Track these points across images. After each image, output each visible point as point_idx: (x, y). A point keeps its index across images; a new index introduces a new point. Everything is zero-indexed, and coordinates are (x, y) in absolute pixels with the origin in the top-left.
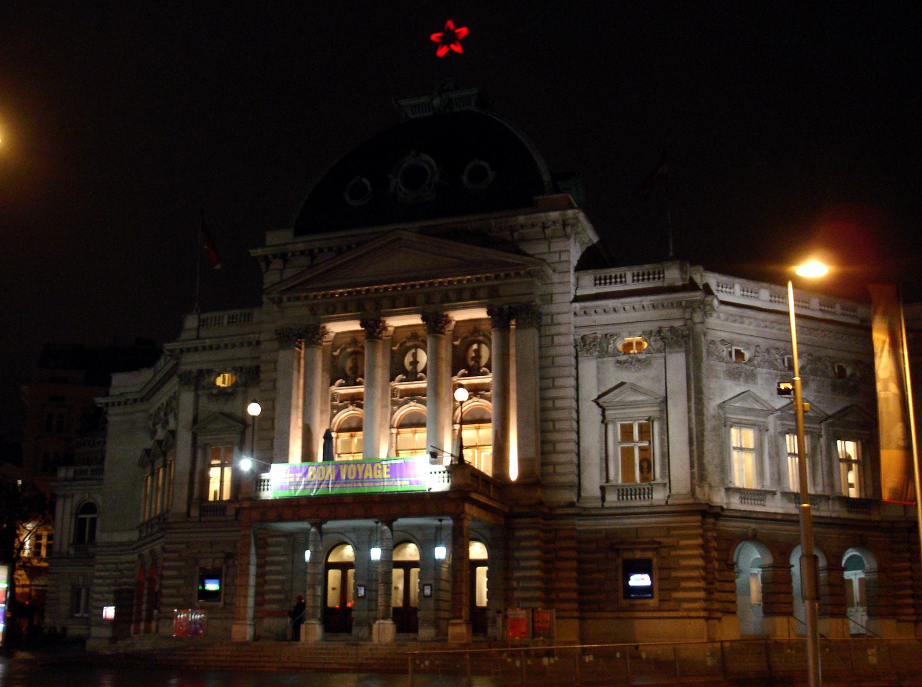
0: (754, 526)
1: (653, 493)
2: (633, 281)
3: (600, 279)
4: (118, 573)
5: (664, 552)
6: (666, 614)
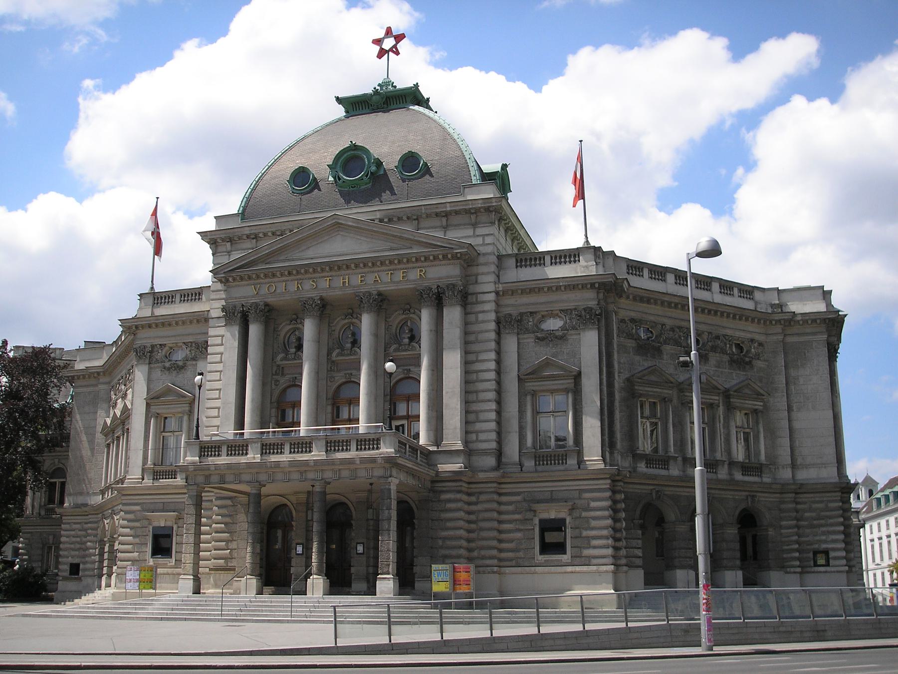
2: (551, 264)
3: (521, 260)
4: (83, 533)
5: (576, 514)
6: (578, 569)
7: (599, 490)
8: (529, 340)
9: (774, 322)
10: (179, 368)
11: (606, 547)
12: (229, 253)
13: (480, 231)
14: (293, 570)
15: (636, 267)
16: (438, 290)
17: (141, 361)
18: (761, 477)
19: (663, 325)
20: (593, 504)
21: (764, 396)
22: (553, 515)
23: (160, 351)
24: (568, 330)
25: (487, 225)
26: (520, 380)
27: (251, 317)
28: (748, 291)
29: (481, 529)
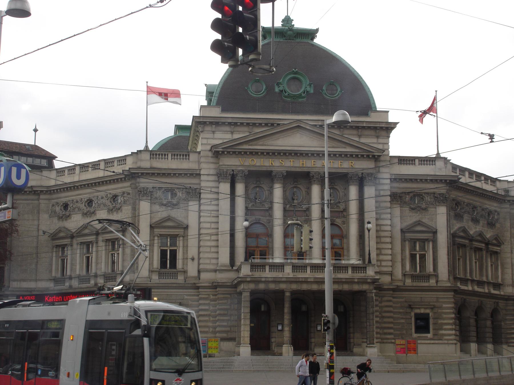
0: (465, 297)
1: (430, 280)
5: (436, 310)
6: (436, 342)
7: (447, 298)
8: (406, 209)
9: (506, 201)
10: (174, 206)
11: (451, 329)
12: (214, 132)
13: (381, 140)
14: (273, 340)
15: (455, 167)
16: (362, 175)
17: (145, 198)
18: (499, 290)
19: (464, 202)
20: (444, 305)
21: (501, 244)
22: (422, 311)
23: (158, 192)
24: (428, 205)
25: (386, 137)
26: (402, 230)
27: (238, 178)
28: (494, 181)
29: (383, 317)
